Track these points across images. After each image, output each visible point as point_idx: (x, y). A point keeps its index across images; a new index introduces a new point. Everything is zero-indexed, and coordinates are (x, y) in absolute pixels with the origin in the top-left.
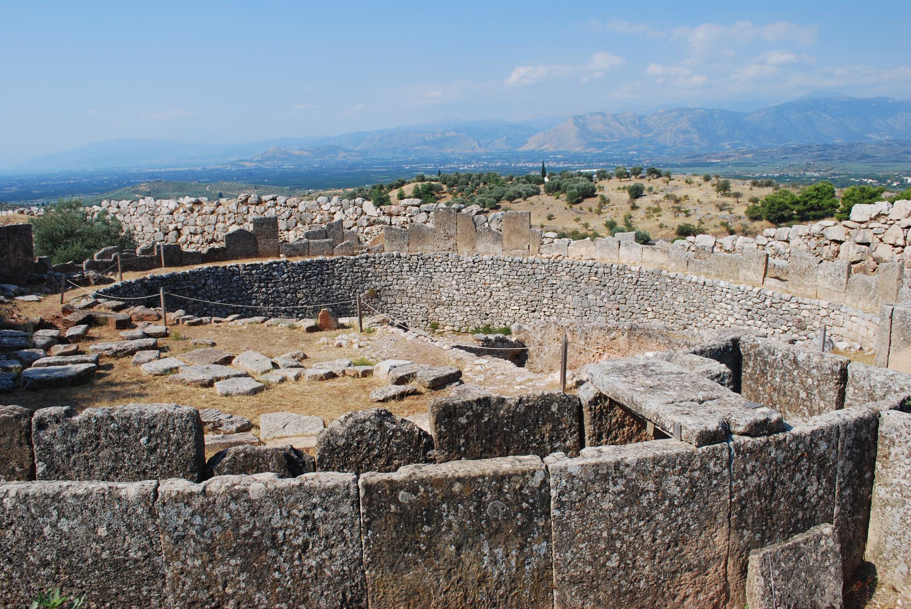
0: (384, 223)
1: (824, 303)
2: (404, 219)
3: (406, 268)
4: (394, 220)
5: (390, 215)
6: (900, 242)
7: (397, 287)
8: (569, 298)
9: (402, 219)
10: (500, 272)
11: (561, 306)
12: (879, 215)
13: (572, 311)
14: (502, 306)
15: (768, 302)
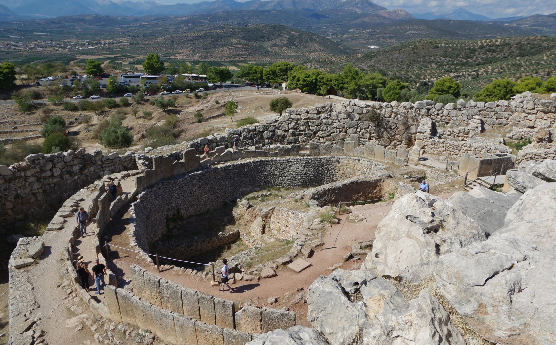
0: (20, 177)
1: (328, 156)
2: (35, 170)
3: (154, 197)
4: (29, 173)
5: (24, 169)
6: (287, 129)
7: (153, 210)
8: (227, 183)
9: (33, 171)
10: (195, 182)
11: (224, 187)
12: (276, 121)
13: (230, 188)
14: (200, 198)
15: (310, 161)
